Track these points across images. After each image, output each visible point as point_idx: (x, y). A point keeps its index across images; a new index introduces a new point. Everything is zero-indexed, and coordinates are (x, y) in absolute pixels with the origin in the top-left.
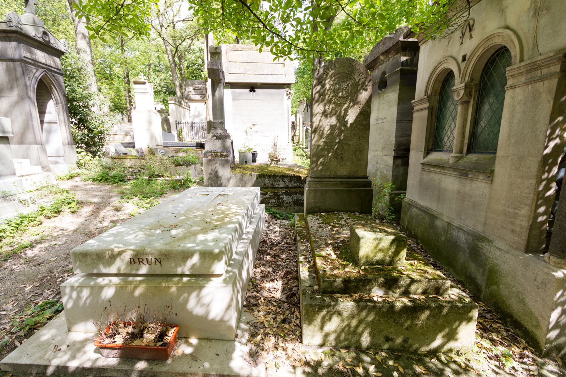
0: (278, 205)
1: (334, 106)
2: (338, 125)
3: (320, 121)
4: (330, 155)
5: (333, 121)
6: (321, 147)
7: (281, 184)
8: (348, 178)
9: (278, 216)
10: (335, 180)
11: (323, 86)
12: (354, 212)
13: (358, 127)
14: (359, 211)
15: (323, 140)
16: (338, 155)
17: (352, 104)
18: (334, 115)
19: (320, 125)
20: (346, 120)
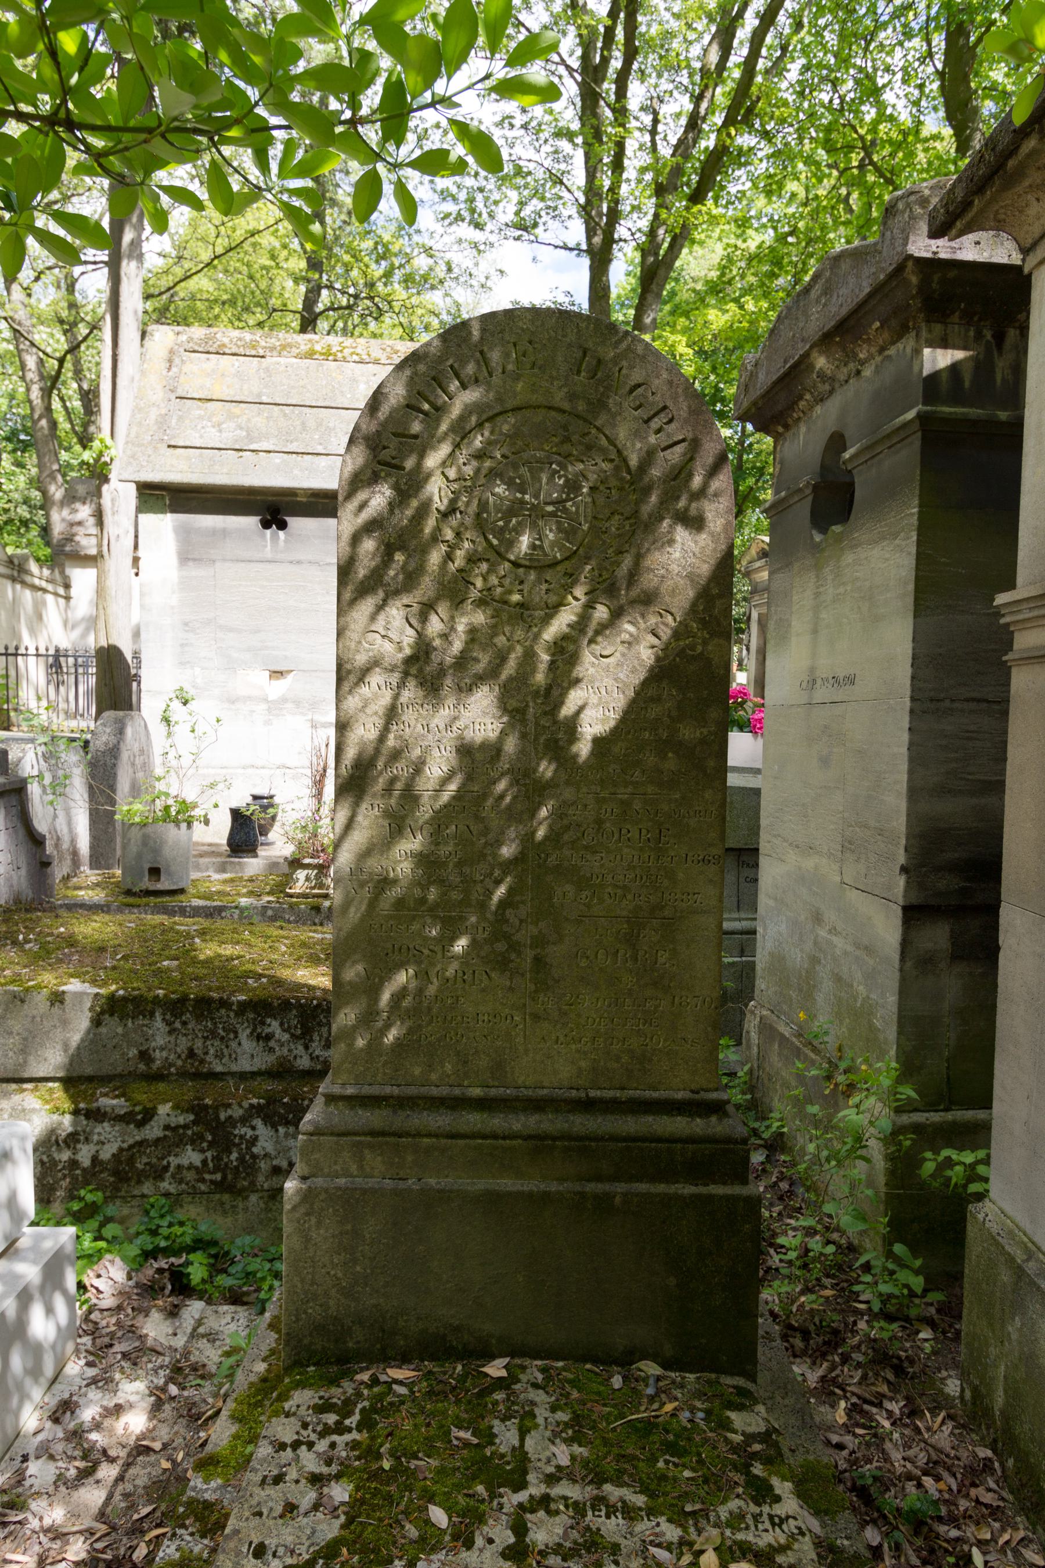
0: (221, 1186)
1: (480, 618)
2: (511, 745)
3: (392, 714)
4: (461, 945)
5: (479, 716)
6: (396, 892)
7: (248, 1055)
8: (588, 1105)
9: (197, 1271)
10: (497, 1122)
11: (409, 486)
12: (626, 1360)
13: (651, 759)
14: (668, 1350)
15: (412, 844)
16: (514, 947)
17: (601, 612)
18: (480, 679)
19: (391, 742)
20: (567, 710)
